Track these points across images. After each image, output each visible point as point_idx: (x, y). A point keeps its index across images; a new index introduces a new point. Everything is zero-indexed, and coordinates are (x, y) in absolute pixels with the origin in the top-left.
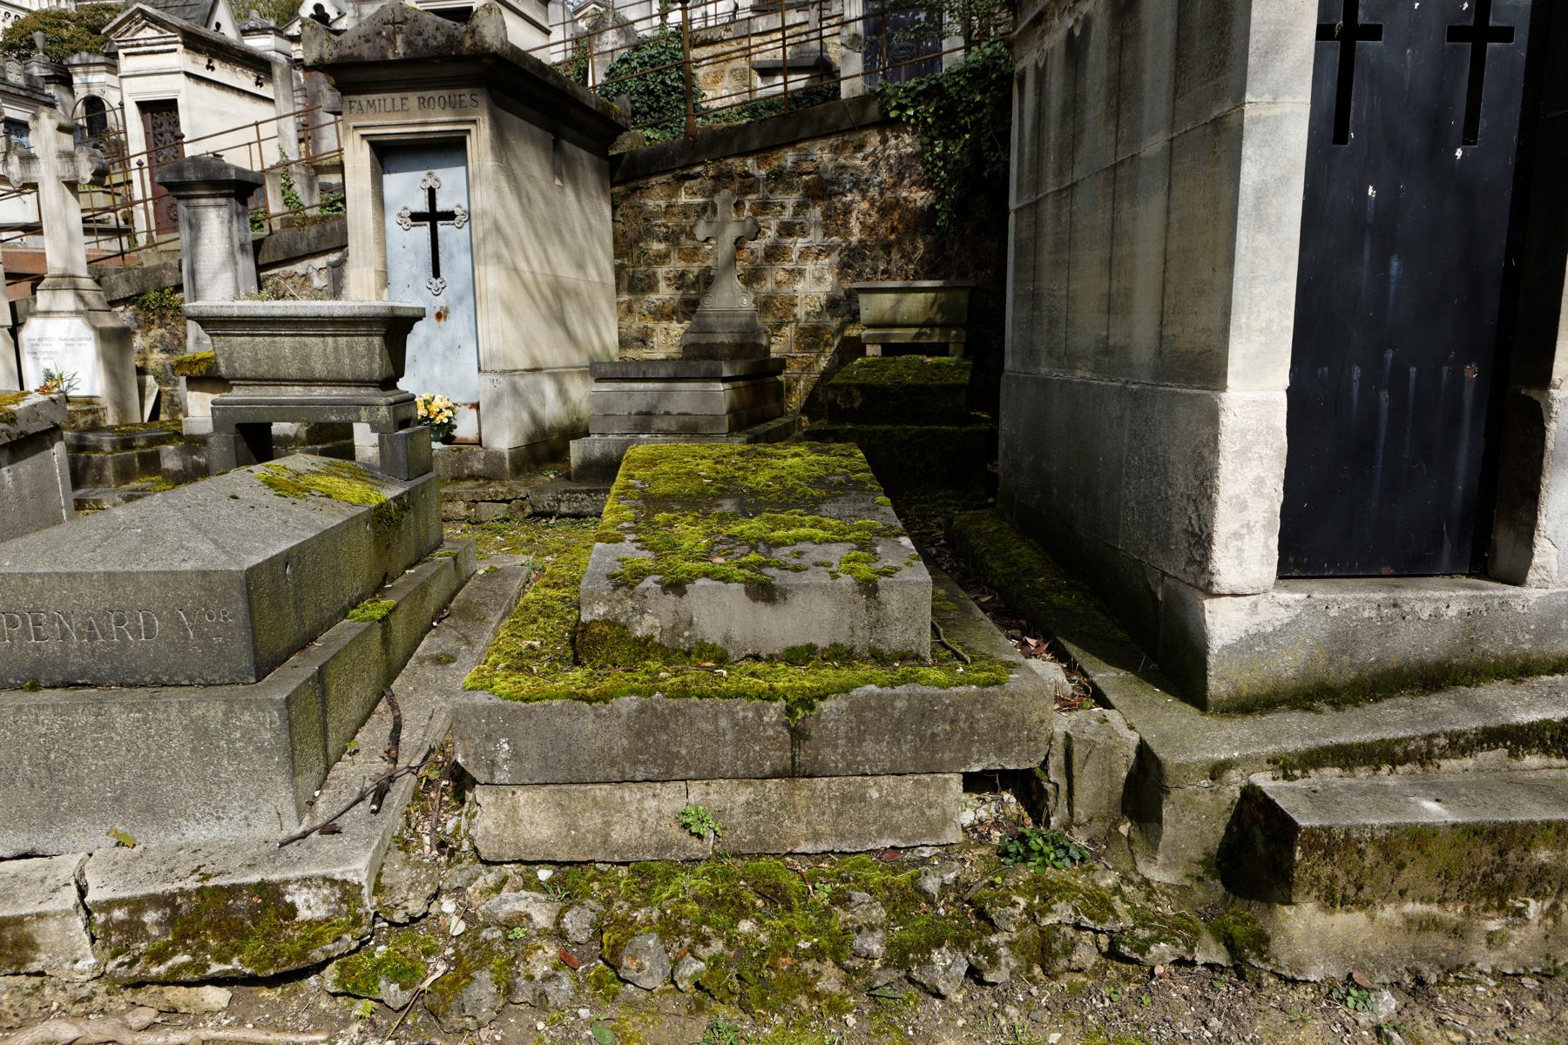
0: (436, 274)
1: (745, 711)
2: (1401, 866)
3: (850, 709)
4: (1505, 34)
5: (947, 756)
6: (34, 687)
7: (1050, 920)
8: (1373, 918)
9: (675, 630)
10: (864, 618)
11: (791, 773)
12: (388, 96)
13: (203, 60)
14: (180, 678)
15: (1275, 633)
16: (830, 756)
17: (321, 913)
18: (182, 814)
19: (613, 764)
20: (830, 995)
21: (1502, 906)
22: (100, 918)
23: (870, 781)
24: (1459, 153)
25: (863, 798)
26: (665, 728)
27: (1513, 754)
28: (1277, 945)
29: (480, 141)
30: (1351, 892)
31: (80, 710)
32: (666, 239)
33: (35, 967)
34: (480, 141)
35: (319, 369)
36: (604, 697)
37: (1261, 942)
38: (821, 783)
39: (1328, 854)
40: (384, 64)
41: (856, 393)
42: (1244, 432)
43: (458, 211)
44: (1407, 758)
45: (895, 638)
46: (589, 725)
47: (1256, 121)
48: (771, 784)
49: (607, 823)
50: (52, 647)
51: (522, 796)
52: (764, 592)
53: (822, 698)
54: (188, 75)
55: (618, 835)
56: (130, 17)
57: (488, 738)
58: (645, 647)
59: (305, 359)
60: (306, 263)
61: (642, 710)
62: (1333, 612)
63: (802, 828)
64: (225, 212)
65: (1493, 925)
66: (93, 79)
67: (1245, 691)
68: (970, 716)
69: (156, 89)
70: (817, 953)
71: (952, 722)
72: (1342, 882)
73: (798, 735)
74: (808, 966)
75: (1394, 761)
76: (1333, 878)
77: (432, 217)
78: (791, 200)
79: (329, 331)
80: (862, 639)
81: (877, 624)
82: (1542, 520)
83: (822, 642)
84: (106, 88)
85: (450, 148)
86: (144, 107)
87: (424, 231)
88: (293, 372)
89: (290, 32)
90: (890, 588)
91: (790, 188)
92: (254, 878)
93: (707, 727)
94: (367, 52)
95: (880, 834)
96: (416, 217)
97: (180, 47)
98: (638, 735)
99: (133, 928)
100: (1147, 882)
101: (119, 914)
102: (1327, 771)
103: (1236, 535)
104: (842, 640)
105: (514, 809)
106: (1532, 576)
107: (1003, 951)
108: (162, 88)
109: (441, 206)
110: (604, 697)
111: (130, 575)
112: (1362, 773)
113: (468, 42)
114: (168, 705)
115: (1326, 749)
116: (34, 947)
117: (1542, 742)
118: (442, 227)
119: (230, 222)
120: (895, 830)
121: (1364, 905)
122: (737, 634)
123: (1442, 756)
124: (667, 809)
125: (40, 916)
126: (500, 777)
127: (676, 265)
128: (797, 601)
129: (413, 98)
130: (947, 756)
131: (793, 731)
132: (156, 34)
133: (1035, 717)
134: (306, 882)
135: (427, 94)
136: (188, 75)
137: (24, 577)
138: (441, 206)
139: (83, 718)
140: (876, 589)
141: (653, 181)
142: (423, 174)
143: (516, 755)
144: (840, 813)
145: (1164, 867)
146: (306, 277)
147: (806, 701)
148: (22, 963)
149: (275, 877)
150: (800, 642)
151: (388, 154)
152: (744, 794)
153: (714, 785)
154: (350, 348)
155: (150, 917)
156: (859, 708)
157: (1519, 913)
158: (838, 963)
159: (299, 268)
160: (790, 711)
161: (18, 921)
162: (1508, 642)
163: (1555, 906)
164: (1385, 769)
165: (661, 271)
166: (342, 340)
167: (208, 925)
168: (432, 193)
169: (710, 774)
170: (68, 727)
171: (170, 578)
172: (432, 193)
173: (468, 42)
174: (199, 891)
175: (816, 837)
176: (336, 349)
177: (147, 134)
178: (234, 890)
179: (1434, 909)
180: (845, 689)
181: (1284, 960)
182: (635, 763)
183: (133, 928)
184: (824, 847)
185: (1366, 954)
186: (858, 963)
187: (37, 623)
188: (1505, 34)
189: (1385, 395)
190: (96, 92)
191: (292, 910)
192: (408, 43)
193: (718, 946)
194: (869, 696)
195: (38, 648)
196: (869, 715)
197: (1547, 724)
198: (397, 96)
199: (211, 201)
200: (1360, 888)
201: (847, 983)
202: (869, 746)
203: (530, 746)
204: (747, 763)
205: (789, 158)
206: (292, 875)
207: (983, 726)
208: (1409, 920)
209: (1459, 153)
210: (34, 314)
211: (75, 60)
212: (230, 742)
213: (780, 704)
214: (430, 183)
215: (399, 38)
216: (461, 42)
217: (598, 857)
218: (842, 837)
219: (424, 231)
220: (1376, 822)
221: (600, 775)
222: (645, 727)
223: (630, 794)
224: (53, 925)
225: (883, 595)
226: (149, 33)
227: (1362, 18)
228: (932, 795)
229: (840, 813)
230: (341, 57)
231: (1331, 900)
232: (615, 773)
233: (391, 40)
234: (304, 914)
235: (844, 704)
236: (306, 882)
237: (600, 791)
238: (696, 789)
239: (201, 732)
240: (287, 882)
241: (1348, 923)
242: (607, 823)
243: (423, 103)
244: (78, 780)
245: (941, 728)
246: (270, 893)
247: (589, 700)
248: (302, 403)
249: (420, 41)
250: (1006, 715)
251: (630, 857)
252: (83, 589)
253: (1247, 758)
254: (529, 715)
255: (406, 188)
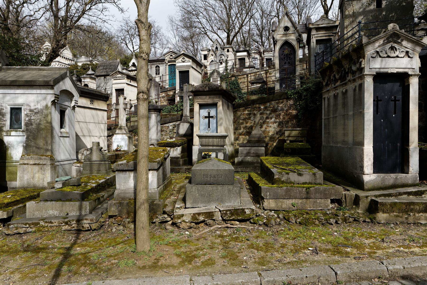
0: (209, 127)
1: (300, 189)
2: (393, 208)
3: (315, 189)
4: (399, 100)
5: (328, 196)
6: (206, 184)
7: (346, 216)
8: (390, 215)
9: (287, 180)
10: (313, 178)
11: (307, 198)
12: (203, 97)
13: (129, 81)
14: (225, 184)
15: (373, 180)
16: (312, 196)
17: (249, 213)
18: (226, 202)
19: (283, 196)
20: (317, 224)
21: (407, 214)
22: (222, 212)
23: (318, 200)
24: (394, 116)
25: (317, 202)
26: (290, 191)
27: (408, 196)
28: (377, 218)
29: (220, 104)
30: (386, 211)
31: (214, 187)
32: (243, 120)
33: (214, 218)
34: (220, 104)
35: (215, 144)
36: (281, 187)
37: (375, 218)
38: (311, 200)
39: (383, 206)
40: (204, 91)
41: (290, 149)
42: (367, 152)
43: (214, 116)
44: (393, 196)
45: (318, 181)
46: (280, 191)
47: (366, 112)
48: (304, 200)
49: (282, 205)
50: (209, 179)
51: (271, 200)
52: (300, 175)
53: (311, 188)
54: (127, 84)
55: (283, 206)
56: (116, 72)
57: (266, 192)
58: (283, 182)
59: (213, 142)
60: (168, 124)
61: (287, 189)
62: (381, 177)
63: (308, 206)
64: (156, 115)
65: (406, 216)
66: (85, 80)
67: (370, 188)
68: (331, 191)
69: (119, 87)
70: (315, 219)
71: (329, 191)
72: (385, 210)
73: (308, 193)
74: (314, 220)
75: (391, 196)
76: (384, 209)
77: (209, 117)
78: (268, 112)
79: (218, 138)
80: (313, 181)
81: (315, 179)
82: (410, 165)
83: (308, 182)
84: (89, 83)
85: (214, 105)
86: (116, 90)
87: (207, 120)
88: (211, 144)
89: (129, 69)
90: (317, 174)
91: (268, 110)
92: (241, 208)
93: (295, 191)
94: (201, 89)
95: (319, 207)
96: (206, 117)
97: (126, 78)
98: (286, 192)
99: (226, 214)
100: (358, 212)
101: (224, 212)
102: (382, 197)
103: (367, 166)
104: (310, 181)
105: (269, 202)
106: (410, 173)
107: (340, 219)
108: (121, 86)
109: (211, 115)
110: (281, 187)
111: (220, 170)
112: (387, 198)
113: (220, 88)
114: (226, 186)
115: (382, 194)
116: (214, 216)
117: (412, 194)
118: (211, 119)
119: (157, 116)
120: (321, 207)
121: (388, 213)
122: (296, 180)
123: (398, 196)
124: (290, 203)
125: (215, 212)
126: (268, 198)
127: (244, 125)
128: (304, 176)
129: (208, 97)
130: (328, 196)
131: (307, 192)
132: (121, 75)
133: (340, 191)
134: (247, 209)
135: (210, 96)
136: (127, 84)
137: (206, 170)
138: (211, 115)
139: (215, 188)
140: (315, 174)
141: (241, 109)
142: (208, 110)
143: (270, 195)
144: (313, 204)
145: (360, 211)
146: (168, 127)
147: (309, 188)
148: (212, 218)
149: (244, 208)
150: (305, 182)
151: (202, 106)
152: (300, 201)
153: (296, 200)
154: (220, 140)
155: (228, 212)
156: (316, 189)
157: (409, 214)
158: (318, 220)
159: (167, 125)
160: (306, 189)
161: (212, 212)
162: (407, 182)
163: (414, 214)
164: (390, 197)
165: (242, 126)
166: (219, 140)
167: (235, 214)
168: (209, 113)
169: (296, 198)
170: (213, 189)
171: (225, 170)
172: (209, 113)
173: (220, 88)
174: (234, 209)
175: (310, 207)
176: (218, 141)
177: (116, 95)
178: (239, 209)
179: (398, 214)
180: (314, 187)
181: (378, 220)
182: (286, 196)
183: (226, 214)
184: (311, 209)
185: (389, 220)
186: (321, 220)
187: (207, 176)
188: (399, 100)
189: (386, 148)
190: (86, 83)
191: (245, 212)
192: (209, 88)
193: (302, 218)
194: (317, 188)
195: (207, 179)
196: (317, 190)
197: (412, 192)
198: (205, 97)
199: (153, 112)
200: (387, 211)
201: (319, 223)
202: (317, 195)
203: (272, 193)
204: (301, 197)
205: (268, 104)
206: (246, 208)
207: (333, 192)
208: (395, 215)
209: (394, 116)
210: (116, 134)
211: (82, 76)
212: (233, 192)
213: (305, 188)
214: (209, 111)
215: (207, 87)
216: (219, 88)
217: (281, 209)
218: (314, 207)
219: (207, 120)
220: (389, 201)
221: (281, 198)
222: (287, 191)
223: (285, 200)
224: (217, 213)
225: (316, 175)
226: (120, 75)
227: (379, 99)
228: (326, 202)
229: (313, 204)
230: (196, 90)
231: (384, 212)
232: (283, 198)
233: (206, 87)
234: (247, 213)
235: (314, 189)
236: (247, 209)
237: (281, 200)
238: (294, 200)
239: (229, 191)
240: (245, 208)
241: (385, 215)
242: (282, 205)
243: (209, 98)
244: (213, 197)
245: (327, 192)
246: (243, 210)
247: (280, 187)
248: (212, 149)
249: (211, 88)
250: (336, 191)
251: (285, 209)
252: (214, 171)
253: (371, 195)
254: (272, 189)
255: (204, 112)
